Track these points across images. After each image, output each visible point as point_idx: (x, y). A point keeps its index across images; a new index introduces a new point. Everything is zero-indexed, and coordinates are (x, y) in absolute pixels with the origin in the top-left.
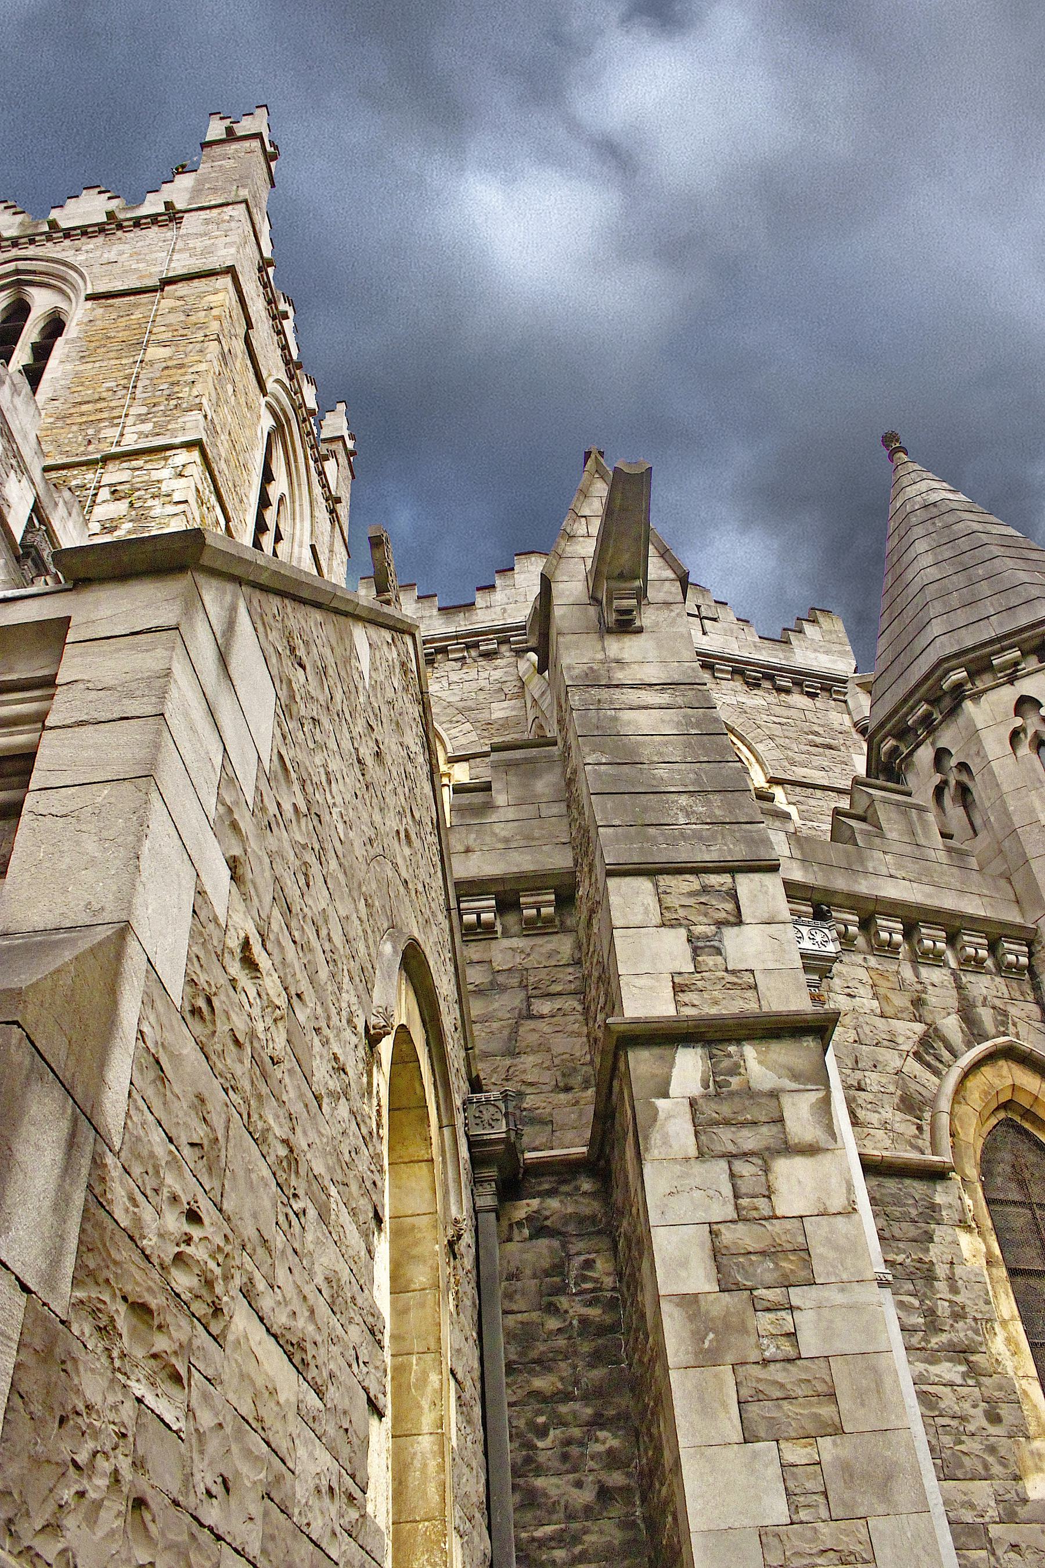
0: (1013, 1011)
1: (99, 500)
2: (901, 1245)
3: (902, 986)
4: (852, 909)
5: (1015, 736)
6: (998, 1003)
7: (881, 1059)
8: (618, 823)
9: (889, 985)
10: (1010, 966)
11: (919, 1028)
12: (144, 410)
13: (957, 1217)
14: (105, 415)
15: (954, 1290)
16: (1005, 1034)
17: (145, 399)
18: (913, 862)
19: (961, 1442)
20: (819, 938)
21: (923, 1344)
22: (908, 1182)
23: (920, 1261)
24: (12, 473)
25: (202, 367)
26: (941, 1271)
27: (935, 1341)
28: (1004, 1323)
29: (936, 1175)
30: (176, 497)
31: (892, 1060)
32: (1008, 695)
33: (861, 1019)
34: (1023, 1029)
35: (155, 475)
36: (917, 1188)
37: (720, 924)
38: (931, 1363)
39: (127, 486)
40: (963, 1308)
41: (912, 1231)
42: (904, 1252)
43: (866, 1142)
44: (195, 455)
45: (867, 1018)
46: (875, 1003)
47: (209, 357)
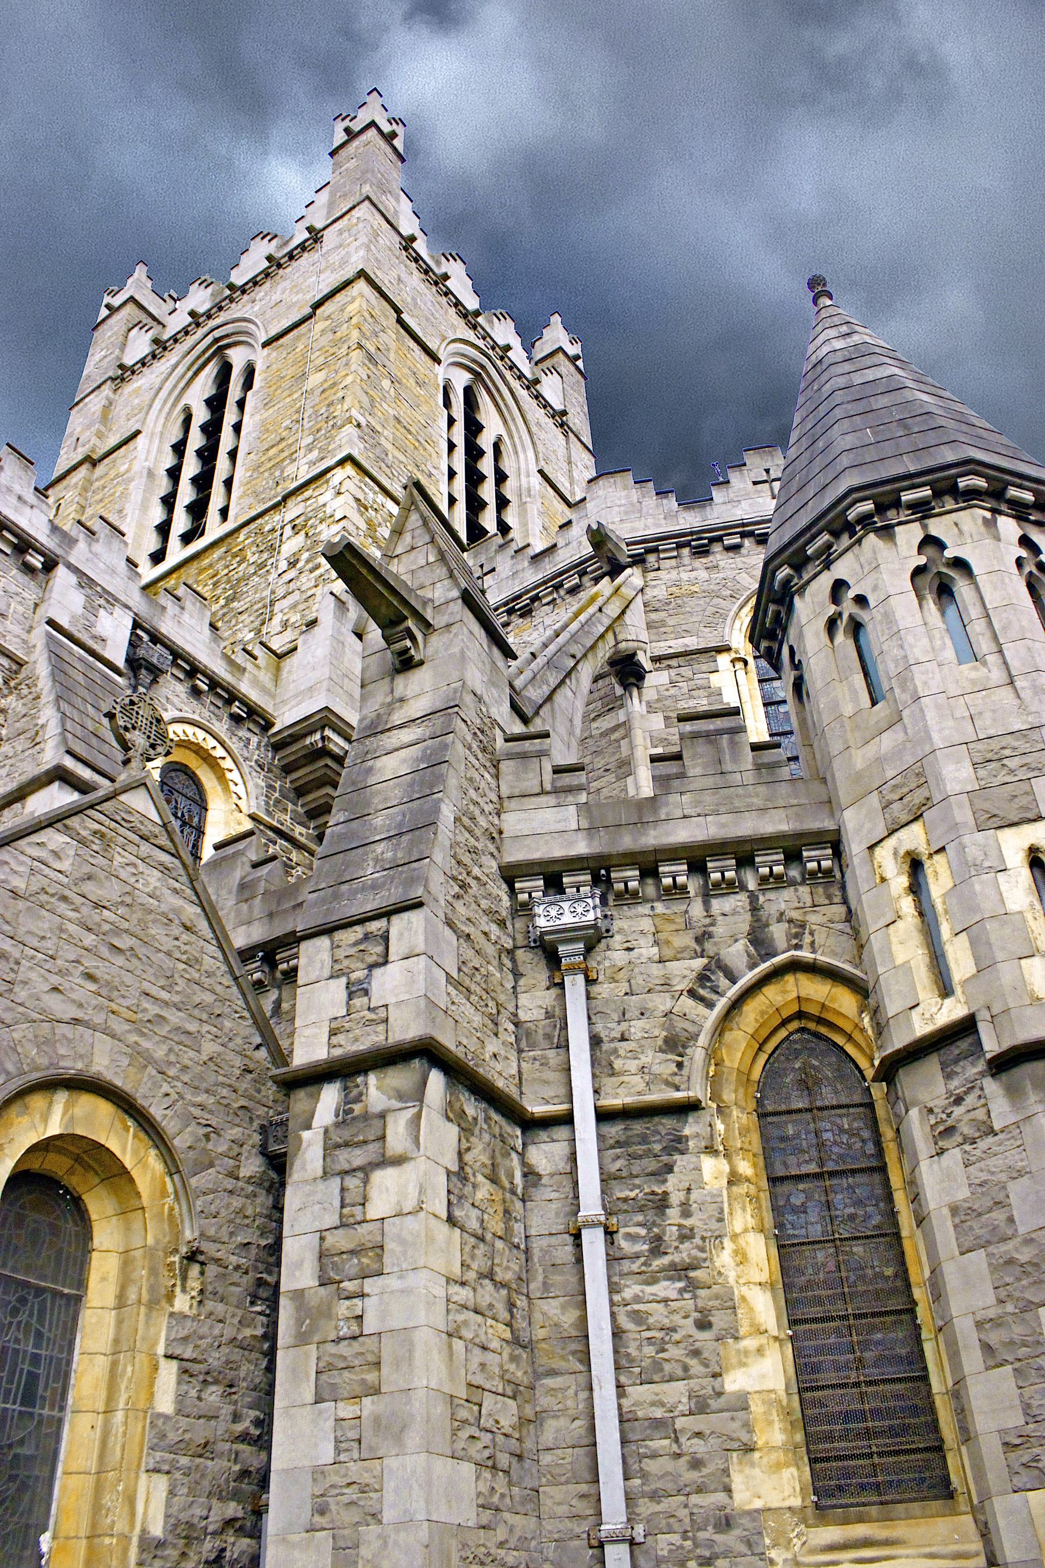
0: (812, 918)
1: (284, 538)
2: (637, 1181)
3: (688, 925)
4: (632, 864)
5: (832, 624)
6: (795, 915)
7: (650, 1005)
8: (323, 885)
9: (674, 927)
10: (813, 874)
11: (699, 963)
12: (310, 439)
13: (703, 1144)
14: (286, 454)
15: (686, 1214)
16: (798, 947)
17: (310, 428)
18: (714, 794)
19: (663, 1350)
20: (580, 910)
21: (643, 1268)
22: (656, 1119)
23: (653, 1193)
24: (102, 612)
25: (349, 380)
26: (676, 1198)
27: (658, 1263)
28: (735, 1237)
29: (689, 1108)
30: (337, 517)
31: (661, 1003)
32: (825, 582)
33: (636, 970)
34: (820, 938)
35: (322, 500)
36: (668, 1123)
37: (372, 967)
38: (649, 1284)
39: (303, 518)
40: (692, 1230)
41: (652, 1165)
42: (638, 1187)
43: (619, 1091)
44: (349, 469)
45: (643, 967)
46: (655, 950)
47: (353, 367)
